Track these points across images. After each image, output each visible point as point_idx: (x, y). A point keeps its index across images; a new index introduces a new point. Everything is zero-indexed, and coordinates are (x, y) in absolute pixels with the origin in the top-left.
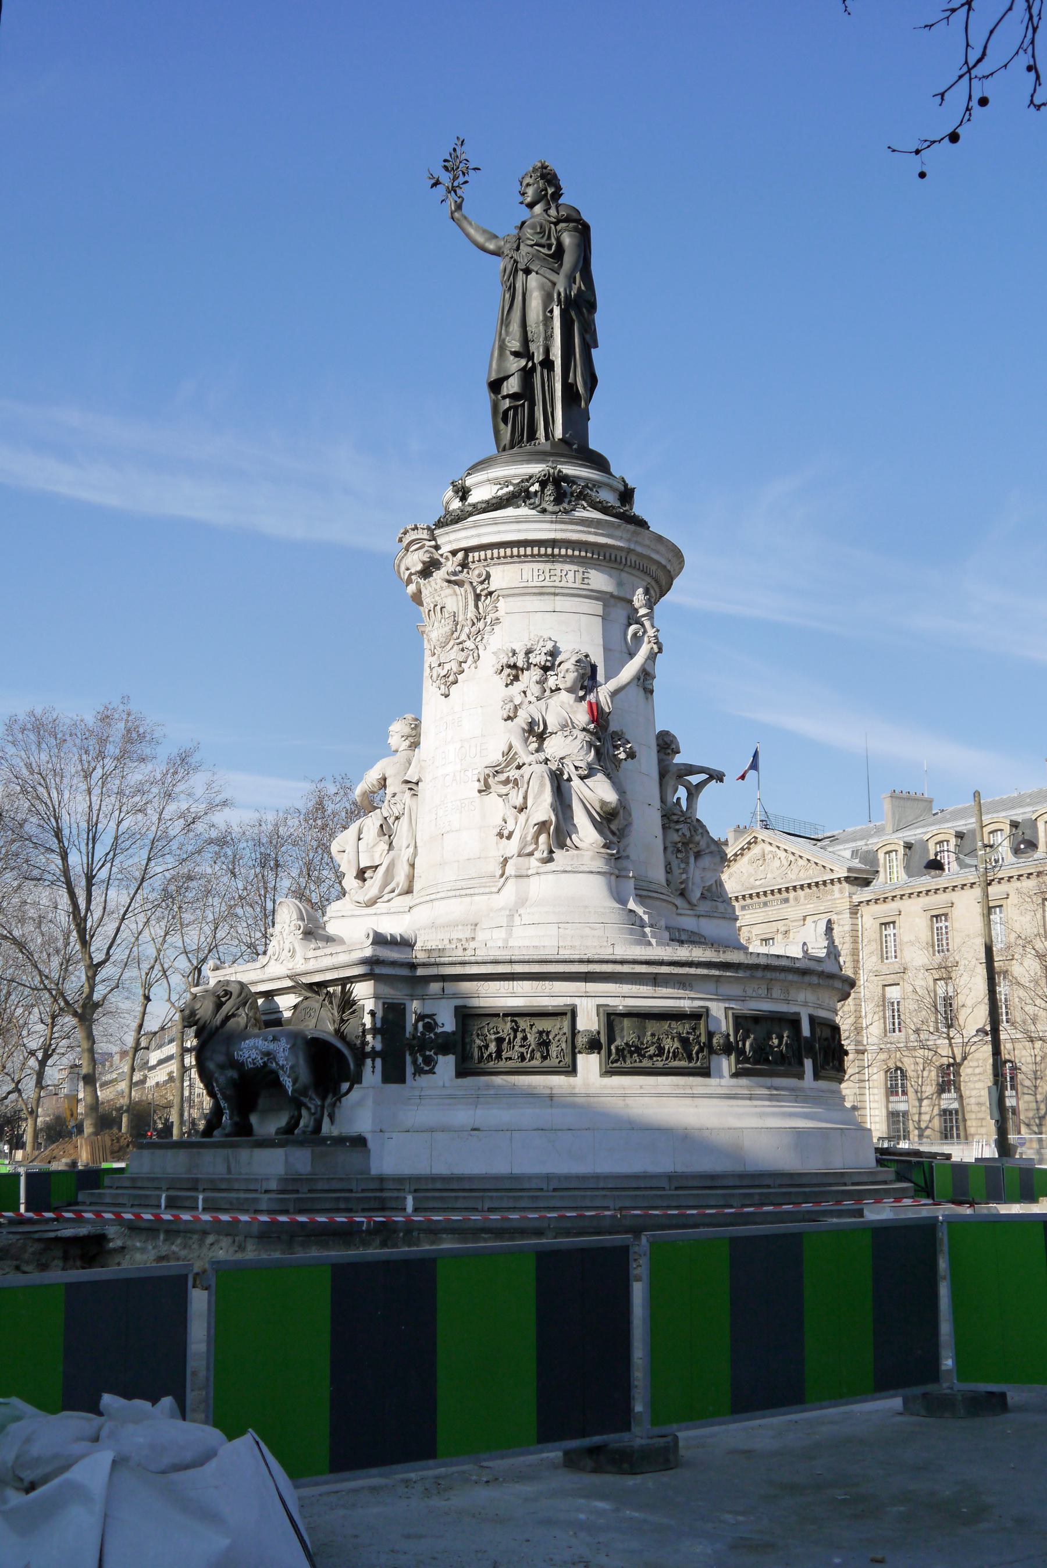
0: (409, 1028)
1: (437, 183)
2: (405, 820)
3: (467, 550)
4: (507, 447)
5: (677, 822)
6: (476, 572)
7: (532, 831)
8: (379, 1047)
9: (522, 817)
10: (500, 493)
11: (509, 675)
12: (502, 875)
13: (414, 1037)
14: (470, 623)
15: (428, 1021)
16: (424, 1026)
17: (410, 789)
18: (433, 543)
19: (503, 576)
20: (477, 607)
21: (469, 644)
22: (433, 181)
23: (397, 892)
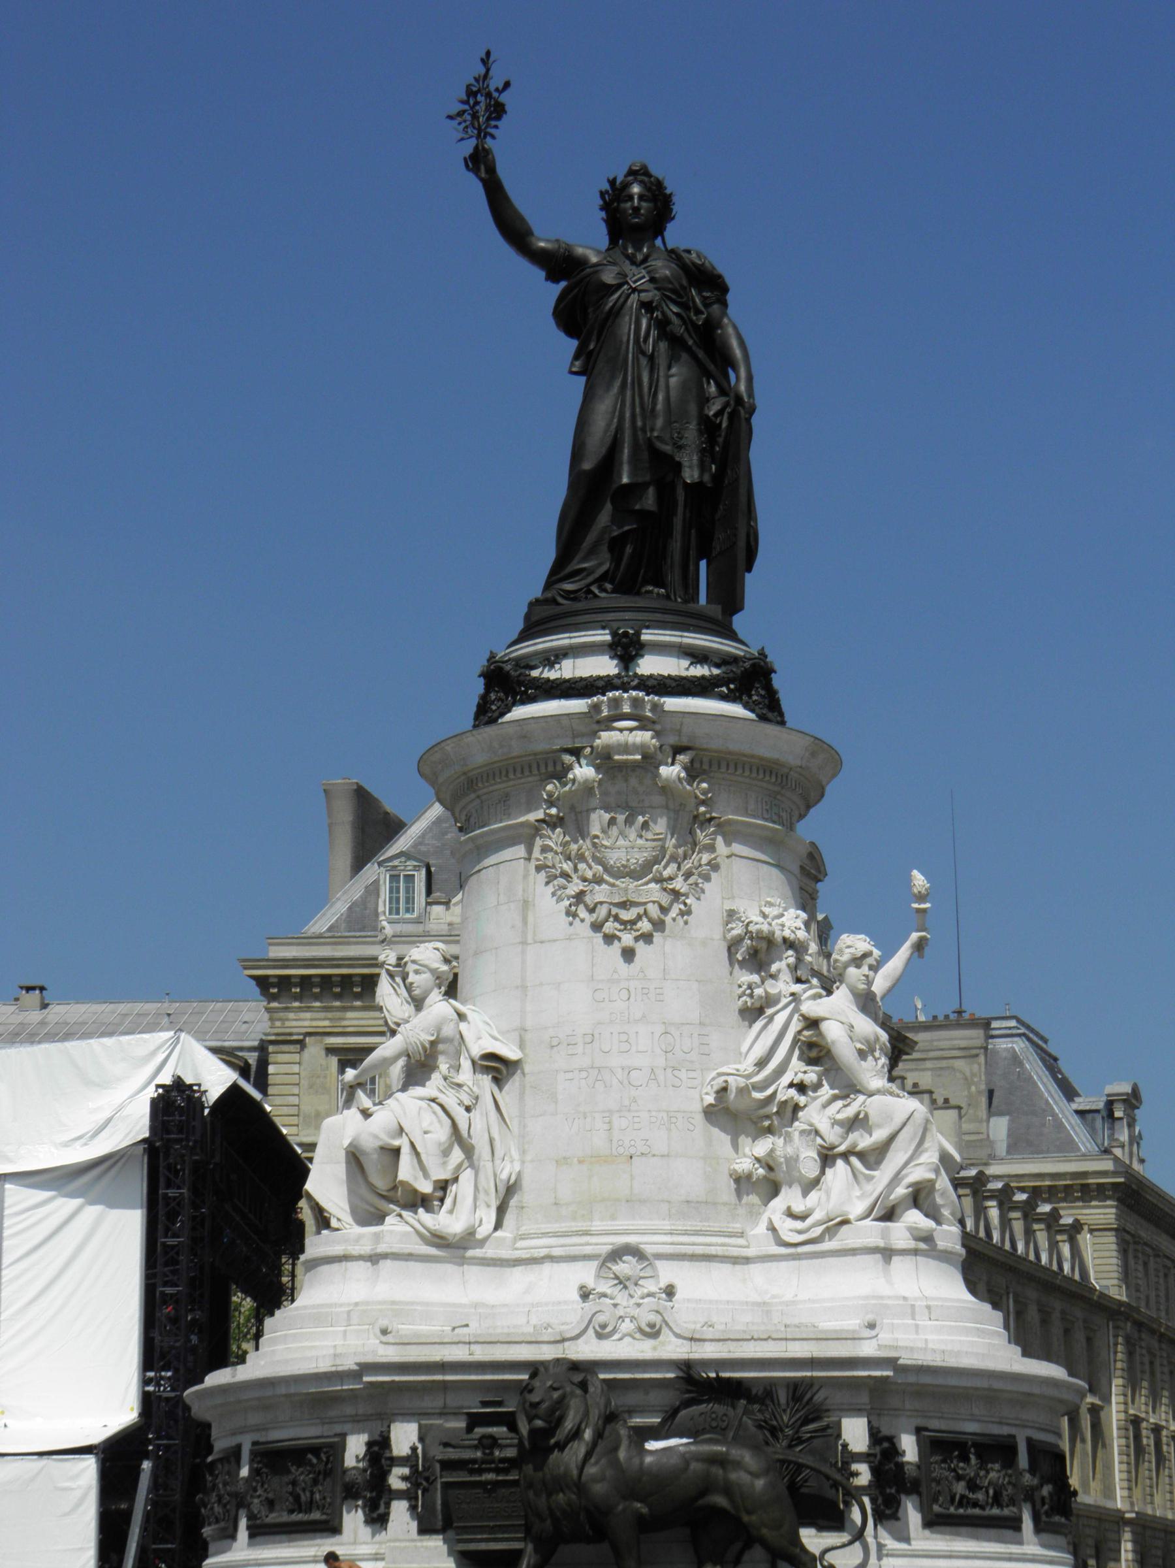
21: (679, 884)
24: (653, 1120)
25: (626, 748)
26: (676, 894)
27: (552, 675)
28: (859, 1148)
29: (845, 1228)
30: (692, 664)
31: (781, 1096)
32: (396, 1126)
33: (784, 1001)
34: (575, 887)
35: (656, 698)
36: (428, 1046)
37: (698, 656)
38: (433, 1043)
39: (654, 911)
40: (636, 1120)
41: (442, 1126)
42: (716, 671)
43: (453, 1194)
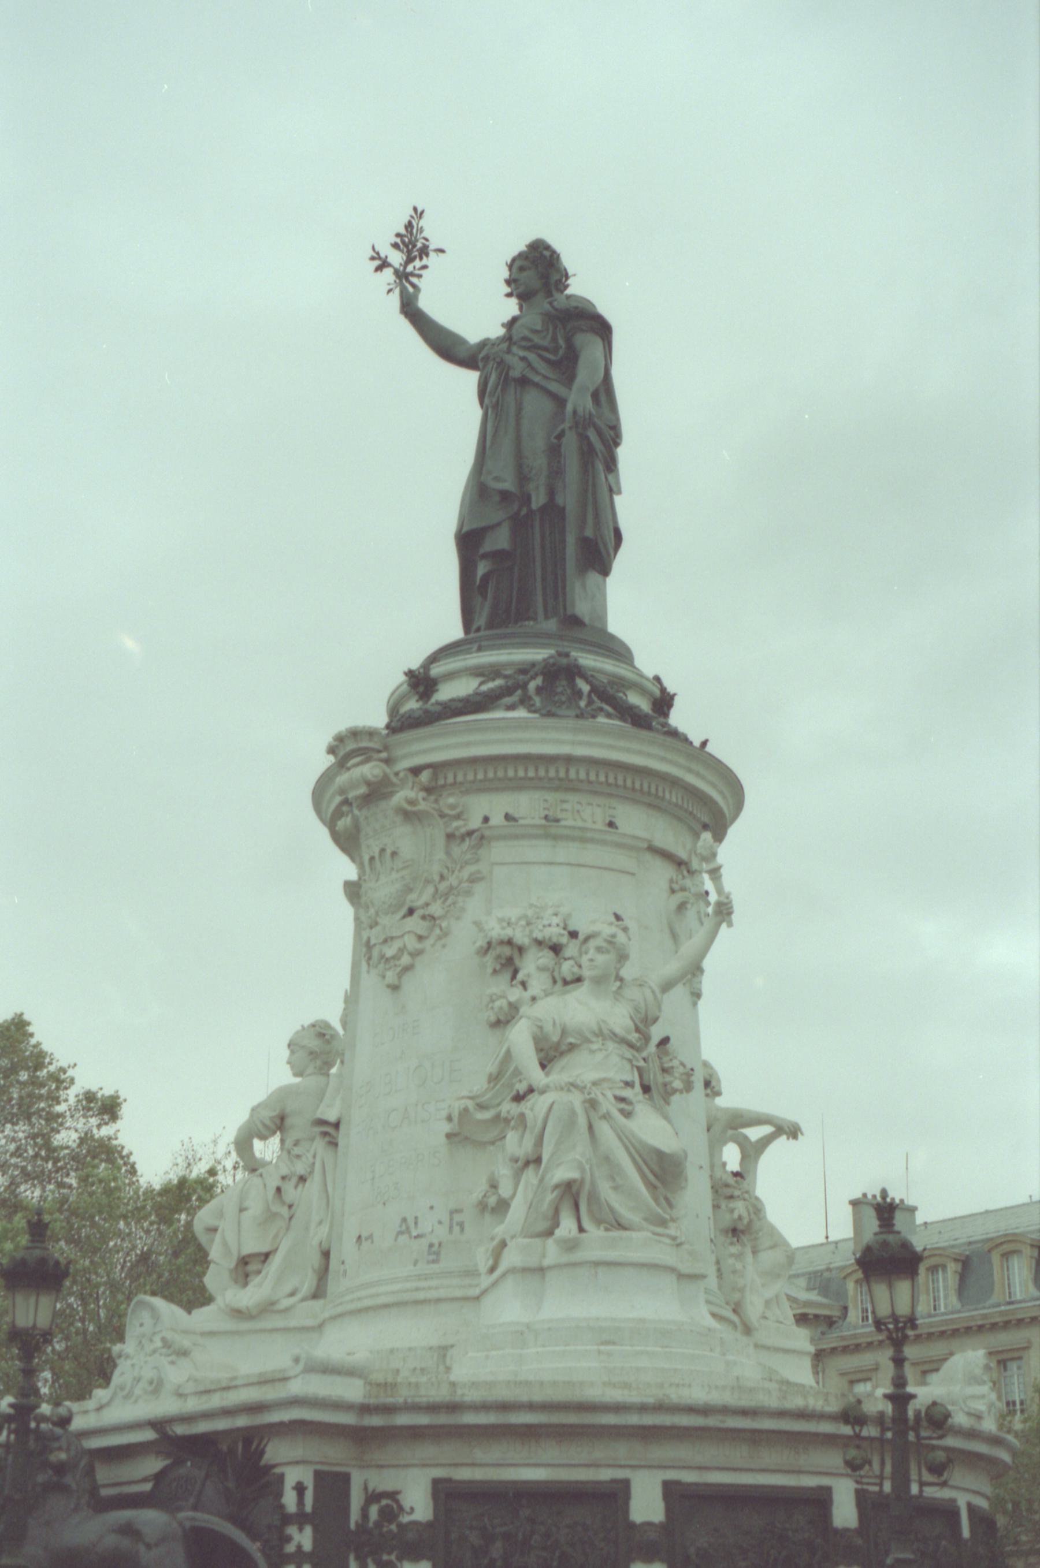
0: (355, 1515)
1: (384, 264)
2: (314, 1185)
3: (436, 768)
4: (483, 628)
5: (731, 1197)
6: (451, 800)
7: (550, 1197)
8: (307, 1545)
9: (530, 1176)
10: (484, 688)
11: (499, 957)
12: (492, 1270)
13: (362, 1526)
14: (437, 878)
15: (389, 1503)
16: (382, 1512)
17: (325, 1134)
18: (384, 755)
19: (487, 807)
20: (448, 853)
21: (436, 909)
22: (377, 263)
23: (299, 1296)
39: (411, 943)
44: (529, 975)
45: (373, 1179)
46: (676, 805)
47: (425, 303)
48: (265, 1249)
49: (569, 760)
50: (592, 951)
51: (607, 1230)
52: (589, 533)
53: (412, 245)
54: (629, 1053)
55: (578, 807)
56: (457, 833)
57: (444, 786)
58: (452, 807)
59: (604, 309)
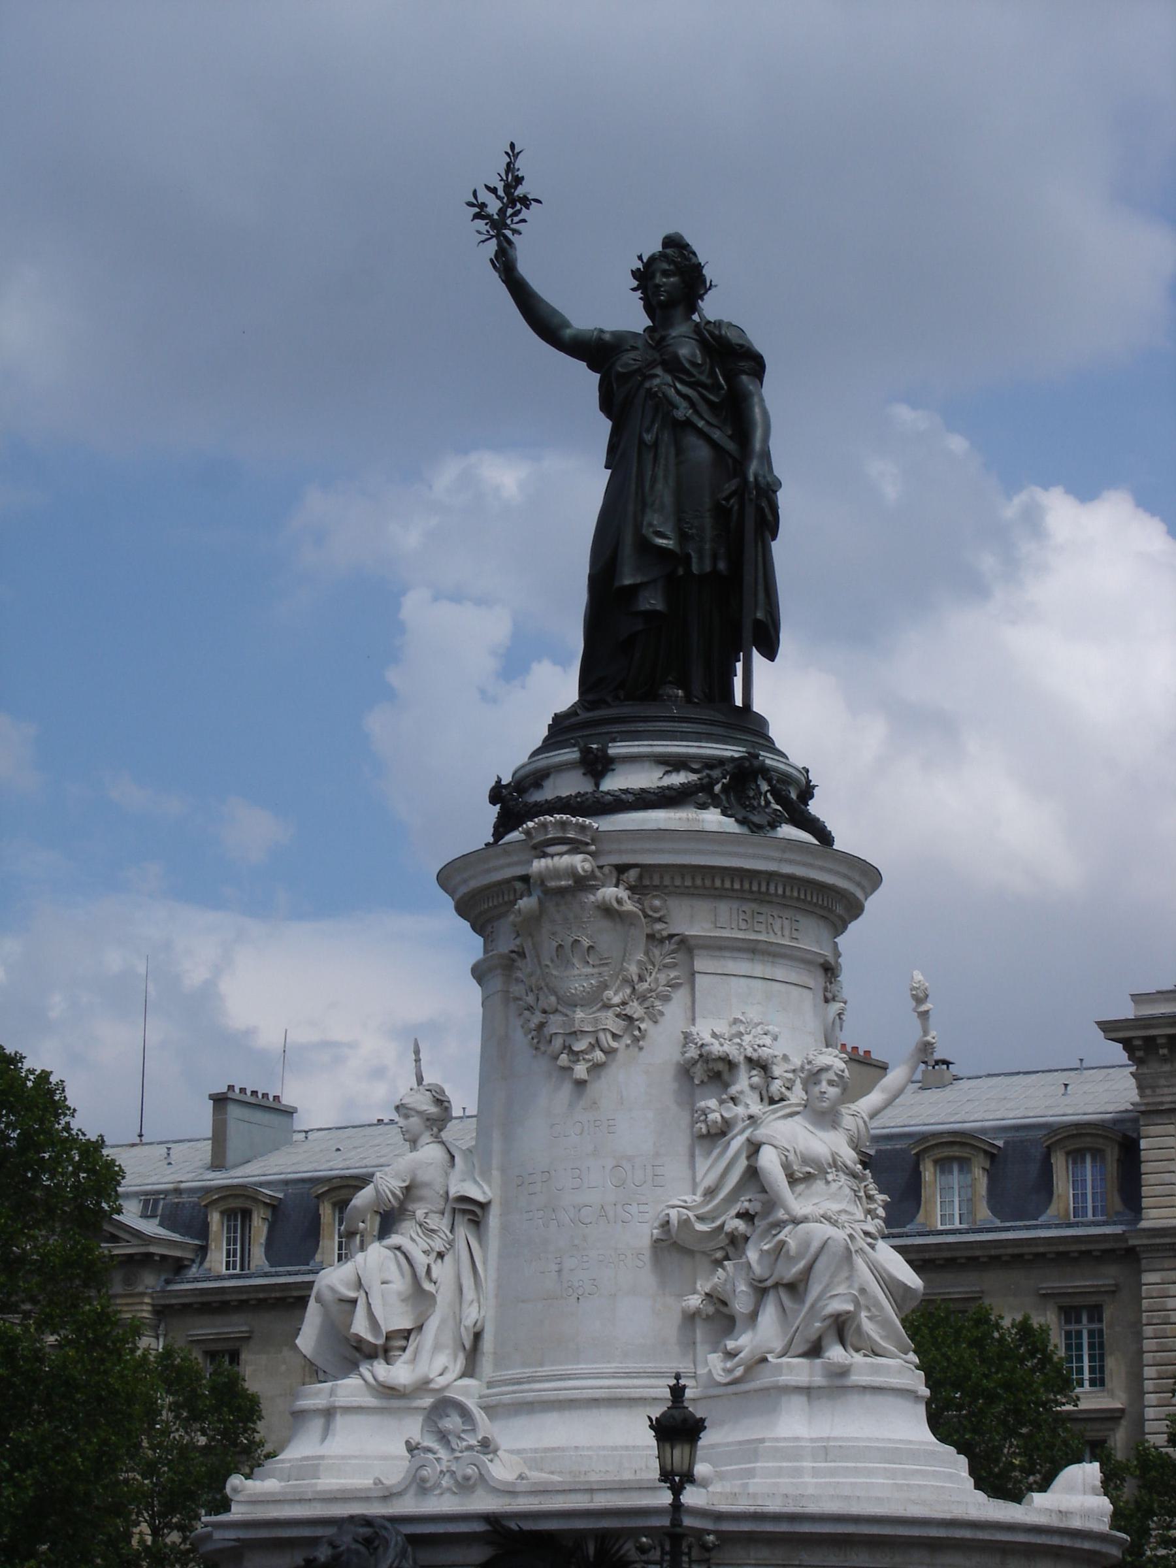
3: (644, 868)
6: (657, 903)
21: (635, 1009)
24: (601, 1258)
25: (556, 874)
26: (629, 1018)
27: (538, 796)
28: (785, 1281)
29: (763, 1365)
30: (666, 773)
31: (728, 1228)
32: (354, 1278)
33: (740, 1125)
34: (537, 1018)
35: (581, 820)
36: (398, 1193)
37: (675, 764)
38: (408, 1188)
40: (585, 1259)
41: (403, 1275)
42: (694, 777)
43: (415, 1345)
44: (742, 1092)
45: (559, 1271)
46: (816, 905)
47: (525, 268)
48: (408, 1325)
49: (771, 876)
50: (824, 1083)
51: (865, 1355)
52: (760, 615)
53: (513, 195)
54: (853, 1183)
55: (770, 920)
56: (658, 936)
57: (656, 887)
58: (656, 910)
59: (760, 346)
